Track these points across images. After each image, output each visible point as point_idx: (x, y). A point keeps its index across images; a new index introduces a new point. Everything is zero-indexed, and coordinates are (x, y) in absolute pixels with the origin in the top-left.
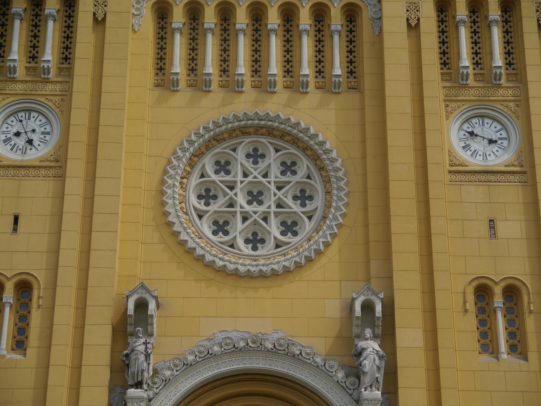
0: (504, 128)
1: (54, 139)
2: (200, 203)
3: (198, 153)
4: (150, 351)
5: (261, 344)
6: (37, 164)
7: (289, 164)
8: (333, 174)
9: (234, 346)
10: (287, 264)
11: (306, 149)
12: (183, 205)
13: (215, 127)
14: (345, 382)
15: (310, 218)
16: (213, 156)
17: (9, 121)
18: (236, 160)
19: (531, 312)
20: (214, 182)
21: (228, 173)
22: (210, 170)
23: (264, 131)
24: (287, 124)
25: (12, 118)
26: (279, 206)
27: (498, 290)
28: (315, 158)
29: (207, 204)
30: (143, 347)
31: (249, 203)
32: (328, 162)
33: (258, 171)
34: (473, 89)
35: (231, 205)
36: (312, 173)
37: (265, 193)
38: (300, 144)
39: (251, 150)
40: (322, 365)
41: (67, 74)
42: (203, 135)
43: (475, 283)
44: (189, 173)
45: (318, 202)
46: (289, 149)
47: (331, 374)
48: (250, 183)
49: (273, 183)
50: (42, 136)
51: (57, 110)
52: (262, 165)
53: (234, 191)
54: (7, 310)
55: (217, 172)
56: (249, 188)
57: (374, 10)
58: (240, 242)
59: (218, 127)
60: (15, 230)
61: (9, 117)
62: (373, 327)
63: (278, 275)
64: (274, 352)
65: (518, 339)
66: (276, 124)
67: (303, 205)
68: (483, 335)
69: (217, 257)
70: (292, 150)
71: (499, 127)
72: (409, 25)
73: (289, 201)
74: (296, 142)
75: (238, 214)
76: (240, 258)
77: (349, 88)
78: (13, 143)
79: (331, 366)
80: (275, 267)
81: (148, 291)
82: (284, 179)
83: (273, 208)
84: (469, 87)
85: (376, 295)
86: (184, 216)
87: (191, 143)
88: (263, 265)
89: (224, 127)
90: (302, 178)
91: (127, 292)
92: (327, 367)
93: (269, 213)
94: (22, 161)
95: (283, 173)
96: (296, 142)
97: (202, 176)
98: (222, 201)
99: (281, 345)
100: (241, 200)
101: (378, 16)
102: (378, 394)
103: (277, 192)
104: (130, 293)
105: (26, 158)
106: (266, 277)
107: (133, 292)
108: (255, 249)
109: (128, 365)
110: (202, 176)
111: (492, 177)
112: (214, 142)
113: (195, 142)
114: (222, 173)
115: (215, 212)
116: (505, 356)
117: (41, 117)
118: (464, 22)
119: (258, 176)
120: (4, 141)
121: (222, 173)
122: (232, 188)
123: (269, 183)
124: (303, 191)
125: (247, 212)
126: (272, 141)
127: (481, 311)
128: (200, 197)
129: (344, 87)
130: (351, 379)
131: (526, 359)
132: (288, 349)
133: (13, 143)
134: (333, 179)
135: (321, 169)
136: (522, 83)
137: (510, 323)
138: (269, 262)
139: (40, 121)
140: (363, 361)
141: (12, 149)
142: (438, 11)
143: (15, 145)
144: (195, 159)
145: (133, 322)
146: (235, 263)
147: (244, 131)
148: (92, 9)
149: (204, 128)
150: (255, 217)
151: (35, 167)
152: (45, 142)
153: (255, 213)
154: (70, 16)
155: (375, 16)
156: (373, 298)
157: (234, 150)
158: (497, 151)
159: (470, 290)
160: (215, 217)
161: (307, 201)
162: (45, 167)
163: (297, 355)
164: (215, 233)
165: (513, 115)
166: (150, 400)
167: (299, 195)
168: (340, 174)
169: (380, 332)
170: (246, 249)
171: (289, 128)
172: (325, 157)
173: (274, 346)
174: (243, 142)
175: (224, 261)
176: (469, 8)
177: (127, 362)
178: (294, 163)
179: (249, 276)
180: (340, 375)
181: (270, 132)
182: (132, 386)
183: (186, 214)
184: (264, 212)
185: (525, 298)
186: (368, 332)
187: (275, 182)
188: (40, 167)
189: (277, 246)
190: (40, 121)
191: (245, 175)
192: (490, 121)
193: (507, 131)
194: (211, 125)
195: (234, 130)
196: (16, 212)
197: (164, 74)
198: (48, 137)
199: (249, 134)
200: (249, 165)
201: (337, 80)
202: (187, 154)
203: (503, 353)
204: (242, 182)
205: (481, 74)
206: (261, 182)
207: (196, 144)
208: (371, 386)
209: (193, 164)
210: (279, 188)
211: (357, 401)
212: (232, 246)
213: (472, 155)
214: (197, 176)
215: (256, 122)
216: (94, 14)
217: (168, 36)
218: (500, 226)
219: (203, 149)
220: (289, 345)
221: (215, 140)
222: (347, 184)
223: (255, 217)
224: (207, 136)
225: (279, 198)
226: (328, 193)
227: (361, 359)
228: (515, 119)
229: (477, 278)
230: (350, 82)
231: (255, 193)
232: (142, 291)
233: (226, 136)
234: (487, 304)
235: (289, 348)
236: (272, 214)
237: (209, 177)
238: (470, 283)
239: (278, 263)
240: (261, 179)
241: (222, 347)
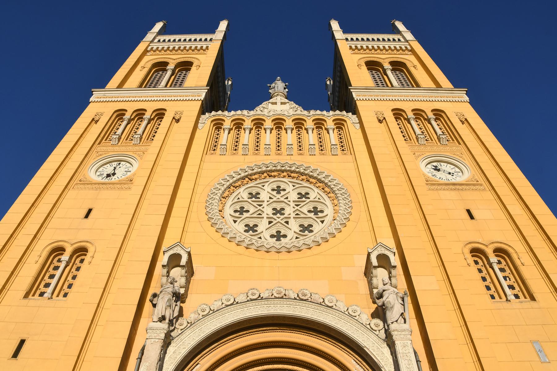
9: (260, 296)
14: (369, 324)
22: (245, 196)
40: (346, 310)
49: (292, 201)
71: (453, 167)
75: (265, 218)
79: (354, 311)
123: (289, 201)
132: (311, 299)
140: (386, 300)
158: (456, 178)
173: (298, 296)
190: (126, 166)
192: (446, 164)
199: (274, 176)
220: (312, 294)
227: (384, 298)
232: (177, 249)
235: (312, 297)
236: (292, 218)
241: (248, 297)
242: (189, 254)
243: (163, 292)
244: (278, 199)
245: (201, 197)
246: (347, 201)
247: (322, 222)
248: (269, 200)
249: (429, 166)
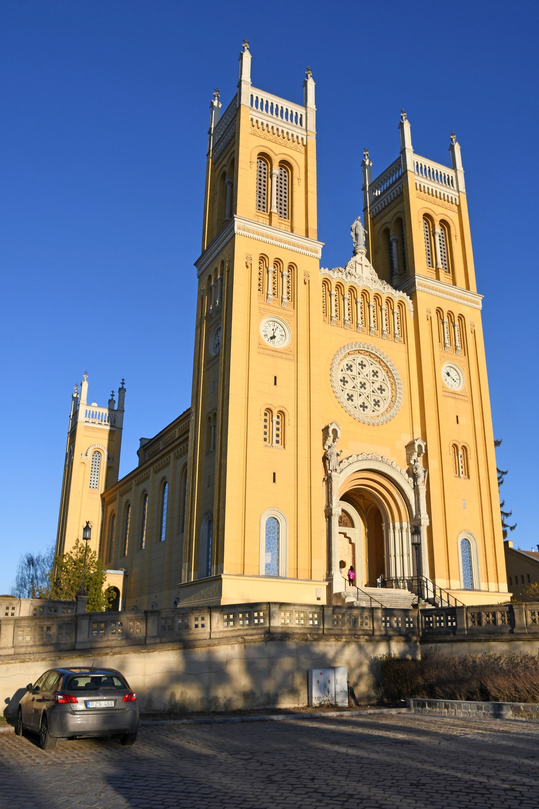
27: (460, 447)
28: (388, 371)
45: (388, 393)
50: (281, 337)
74: (380, 361)
96: (380, 361)
110: (342, 370)
111: (457, 396)
141: (268, 341)
148: (303, 277)
159: (451, 445)
181: (370, 354)
189: (373, 411)
198: (284, 338)
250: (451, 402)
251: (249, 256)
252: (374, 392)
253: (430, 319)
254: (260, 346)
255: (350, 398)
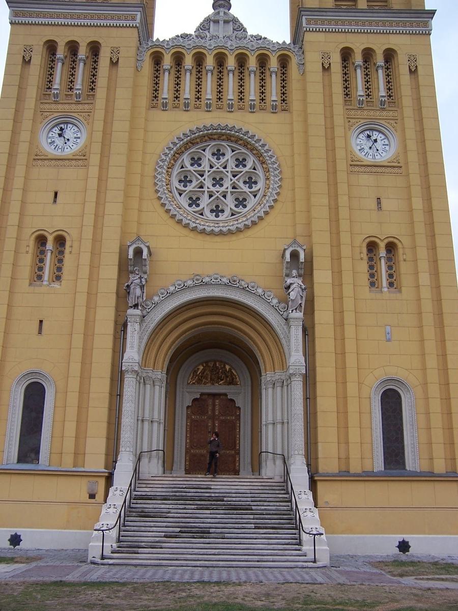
0: (386, 137)
1: (81, 142)
2: (180, 185)
3: (179, 151)
4: (144, 283)
5: (220, 280)
6: (71, 157)
7: (241, 160)
8: (271, 166)
9: (202, 281)
10: (239, 226)
11: (252, 149)
12: (169, 186)
13: (191, 134)
15: (255, 196)
16: (190, 154)
17: (54, 130)
18: (206, 156)
19: (405, 260)
20: (190, 171)
21: (200, 165)
22: (187, 163)
23: (224, 137)
24: (240, 133)
25: (56, 128)
26: (234, 188)
28: (259, 156)
29: (185, 186)
30: (139, 281)
31: (214, 185)
32: (268, 158)
33: (220, 164)
34: (366, 111)
35: (202, 187)
36: (257, 165)
37: (224, 179)
38: (249, 146)
39: (216, 151)
41: (92, 98)
42: (183, 140)
43: (368, 240)
44: (173, 165)
45: (260, 185)
46: (241, 150)
47: (268, 301)
48: (214, 172)
49: (229, 172)
50: (75, 140)
51: (85, 122)
52: (223, 160)
53: (203, 178)
54: (49, 254)
55: (192, 165)
56: (214, 176)
57: (299, 58)
58: (207, 212)
59: (193, 134)
60: (55, 201)
61: (53, 127)
62: (298, 269)
63: (233, 234)
64: (231, 284)
65: (394, 279)
66: (233, 132)
67: (250, 187)
68: (372, 275)
69: (191, 221)
70: (243, 151)
72: (323, 67)
73: (241, 184)
74: (246, 145)
75: (206, 192)
76: (207, 222)
77: (283, 110)
78: (55, 144)
80: (231, 228)
81: (143, 242)
82: (237, 169)
83: (230, 189)
84: (364, 110)
85: (301, 247)
86: (170, 194)
87: (175, 144)
88: (223, 227)
89: (197, 134)
90: (250, 169)
91: (128, 243)
92: (266, 296)
93: (227, 192)
94: (61, 156)
95: (237, 166)
96: (246, 145)
97: (182, 167)
98: (194, 183)
99: (234, 281)
100: (208, 183)
101: (303, 63)
102: (300, 315)
103: (232, 178)
104: (131, 244)
105: (63, 154)
106: (225, 235)
107: (133, 243)
108: (217, 216)
109: (129, 292)
110: (182, 167)
111: (379, 170)
112: (190, 144)
113: (177, 144)
114: (196, 165)
115: (190, 191)
116: (385, 290)
117: (74, 127)
118: (361, 66)
119: (219, 167)
120: (50, 143)
121: (196, 165)
122: (202, 176)
123: (227, 172)
124: (250, 178)
125: (212, 192)
126: (230, 144)
127: (371, 259)
128: (180, 181)
129: (279, 108)
130: (283, 305)
131: (400, 291)
133: (55, 144)
134: (271, 170)
135: (263, 163)
136: (398, 107)
137: (390, 267)
138: (226, 225)
139: (74, 130)
141: (55, 149)
142: (342, 60)
143: (57, 145)
144: (177, 155)
145: (132, 263)
146: (203, 225)
147: (211, 137)
148: (109, 55)
149: (183, 134)
150: (217, 194)
151: (68, 159)
152: (76, 143)
153: (218, 192)
154: (95, 62)
155: (300, 63)
156: (299, 249)
157: (204, 150)
158: (382, 153)
159: (365, 245)
160: (191, 195)
161: (253, 185)
162: (76, 160)
163: (246, 288)
164: (190, 205)
165: (393, 129)
166: (144, 317)
167: (248, 180)
168: (275, 166)
169: (303, 273)
170: (212, 217)
171: (242, 135)
172: (265, 154)
174: (209, 145)
175: (196, 224)
176: (364, 58)
177: (128, 291)
178: (244, 160)
179: (212, 233)
180: (275, 301)
181: (229, 138)
182: (131, 307)
183: (171, 192)
184: (224, 192)
185: (401, 251)
186: (294, 272)
187: (231, 172)
188: (72, 160)
189: (233, 215)
190: (74, 130)
191: (211, 167)
193: (388, 139)
194: (188, 132)
195: (204, 137)
196: (56, 189)
197: (157, 100)
198: (79, 140)
199: (214, 139)
200: (214, 160)
201: (274, 104)
202: (172, 152)
203: (385, 287)
204: (209, 171)
205: (371, 102)
206: (222, 172)
207: (178, 145)
208: (296, 309)
209: (176, 159)
210: (234, 176)
211: (286, 320)
212: (202, 214)
213: (365, 155)
214: (178, 167)
215: (219, 131)
216: (111, 58)
217: (161, 75)
218: (384, 202)
219: (183, 149)
221: (191, 143)
222: (281, 172)
223: (217, 194)
224: (185, 140)
225: (234, 182)
226: (267, 179)
227: (290, 290)
228: (394, 132)
229: (369, 237)
230: (283, 106)
231: (218, 179)
233: (198, 140)
234: (375, 255)
236: (229, 192)
237: (187, 168)
238: (364, 240)
239: (233, 225)
240: (222, 169)
242: (148, 247)
243: (133, 284)
244: (218, 168)
245: (149, 170)
246: (278, 178)
247: (255, 196)
248: (209, 169)
249: (361, 136)
250: (365, 179)
251: (28, 48)
252: (236, 189)
253: (326, 69)
254: (38, 157)
255: (194, 202)
